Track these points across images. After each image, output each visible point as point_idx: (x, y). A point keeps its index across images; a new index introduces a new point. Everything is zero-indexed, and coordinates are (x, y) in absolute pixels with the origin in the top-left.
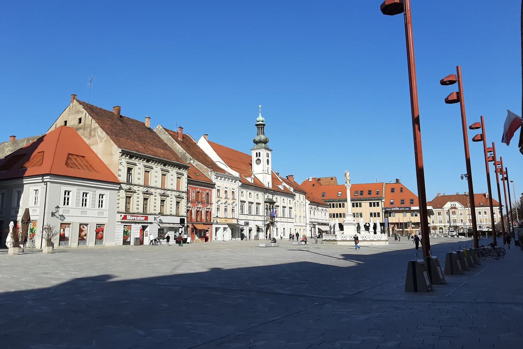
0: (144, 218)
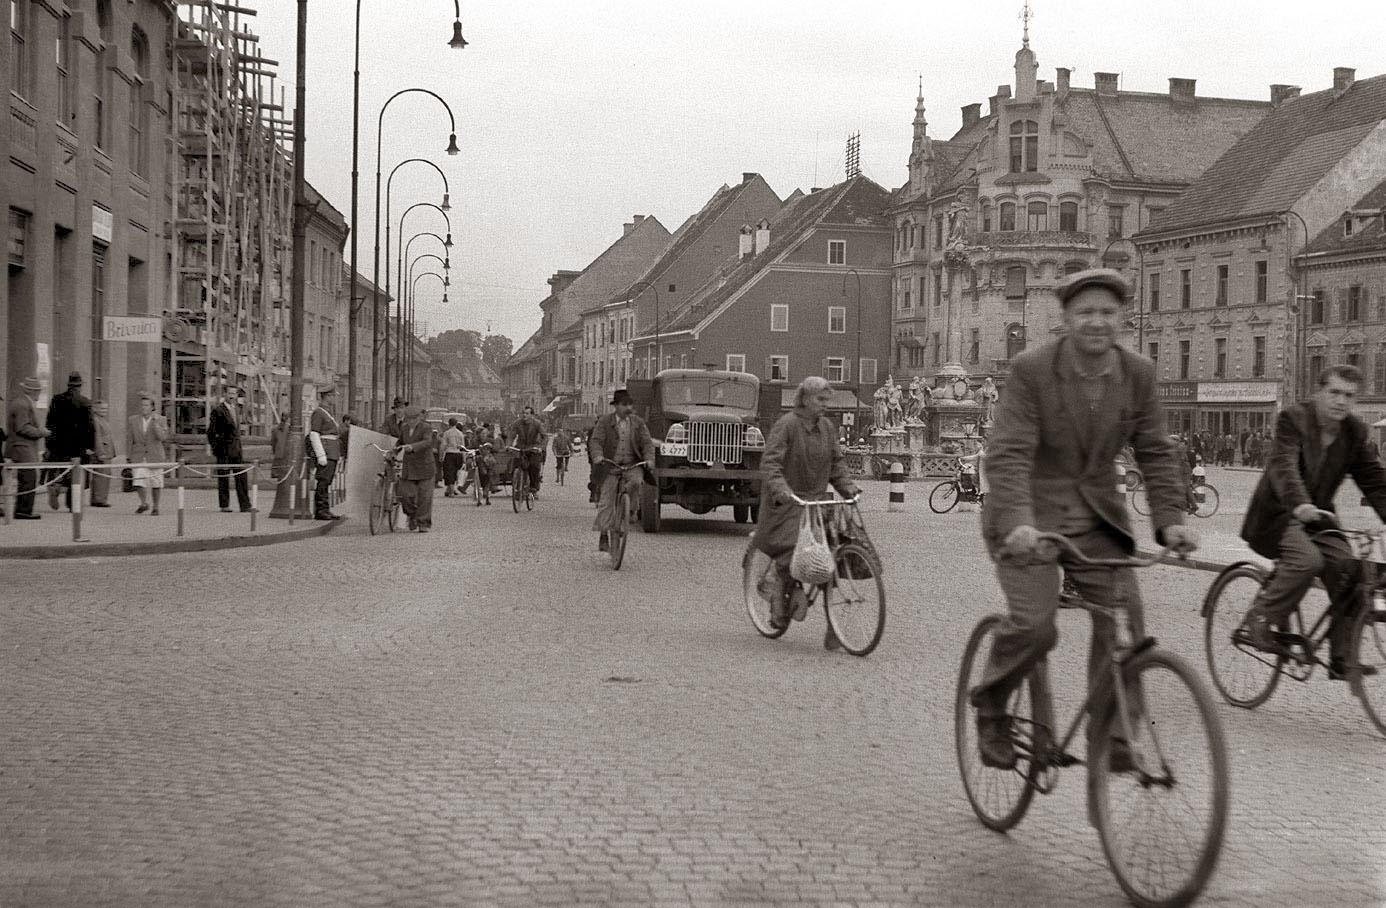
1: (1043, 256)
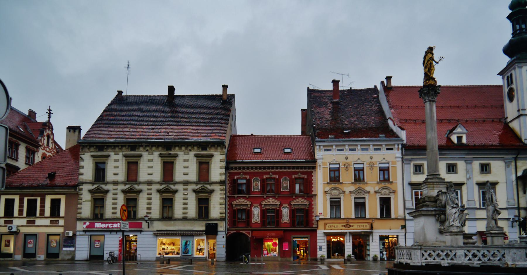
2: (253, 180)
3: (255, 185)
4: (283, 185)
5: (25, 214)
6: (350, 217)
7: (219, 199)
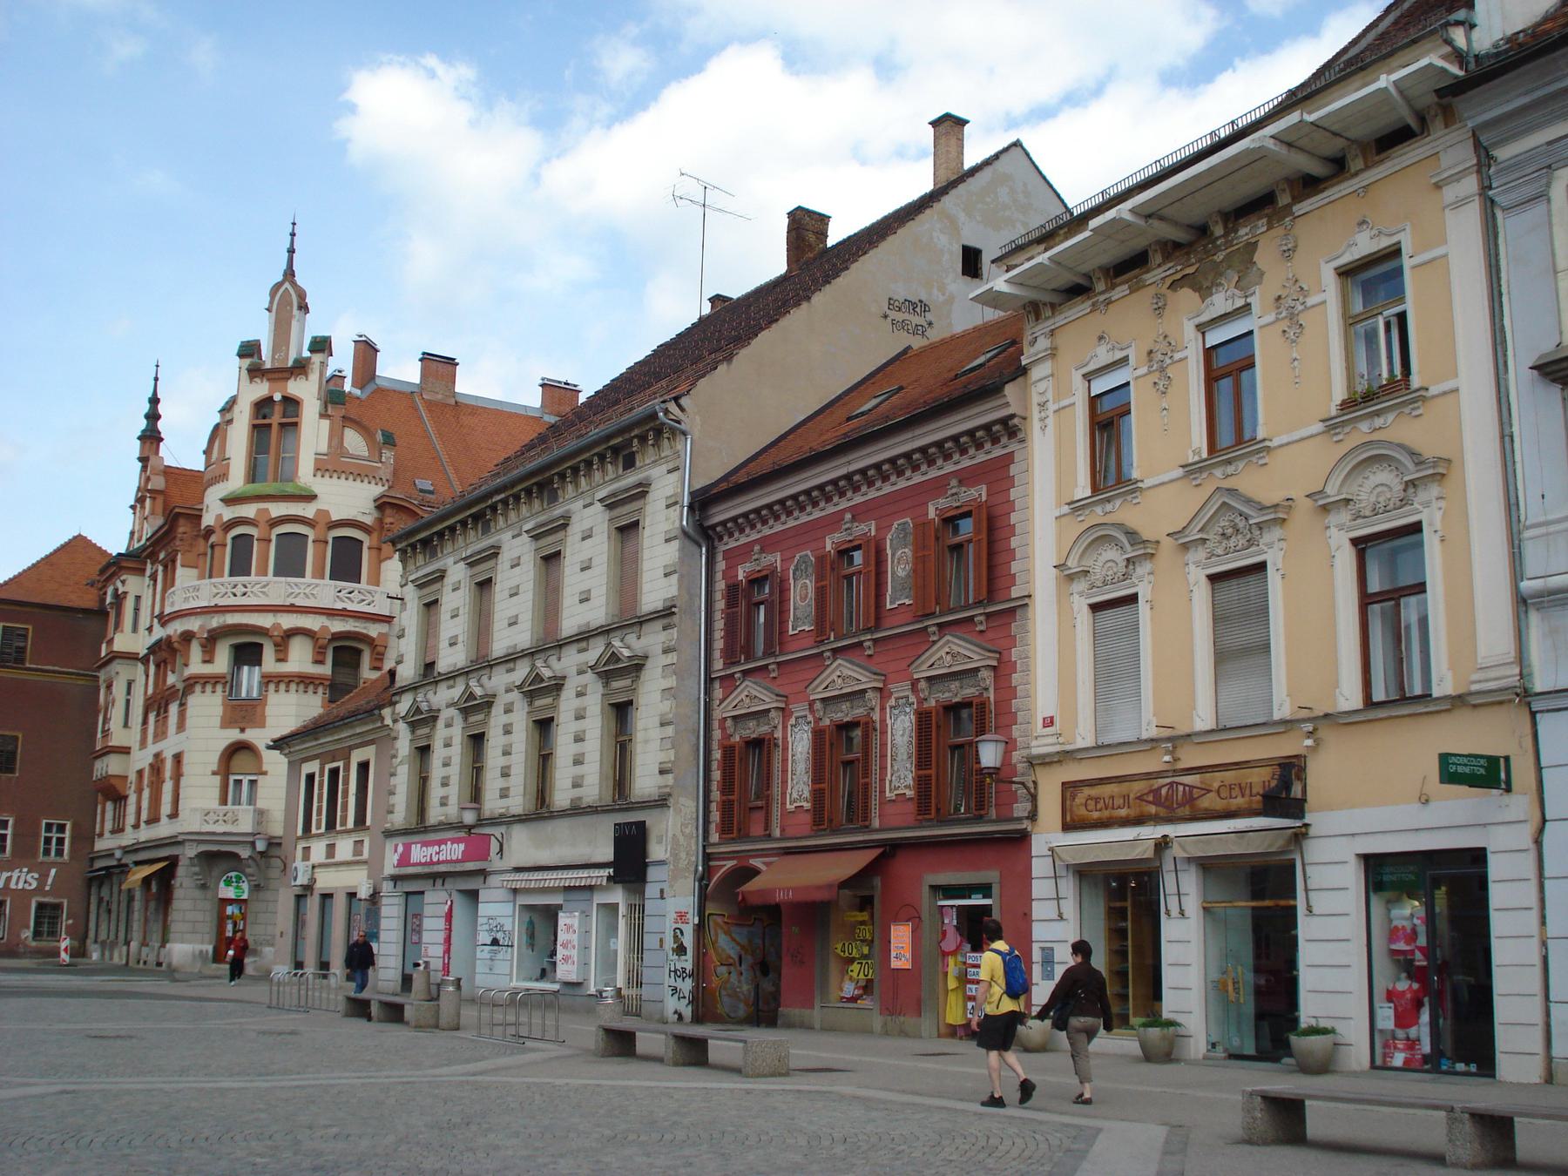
0: (462, 847)
1: (288, 621)
2: (794, 574)
3: (801, 598)
4: (893, 573)
5: (323, 830)
6: (1183, 729)
7: (658, 696)
